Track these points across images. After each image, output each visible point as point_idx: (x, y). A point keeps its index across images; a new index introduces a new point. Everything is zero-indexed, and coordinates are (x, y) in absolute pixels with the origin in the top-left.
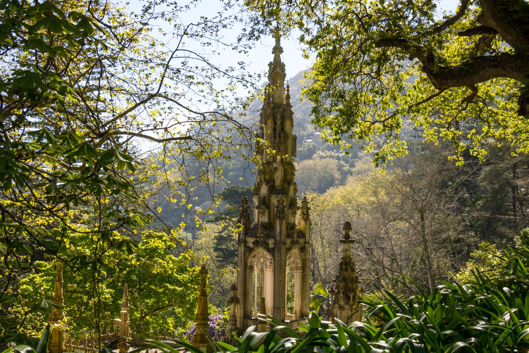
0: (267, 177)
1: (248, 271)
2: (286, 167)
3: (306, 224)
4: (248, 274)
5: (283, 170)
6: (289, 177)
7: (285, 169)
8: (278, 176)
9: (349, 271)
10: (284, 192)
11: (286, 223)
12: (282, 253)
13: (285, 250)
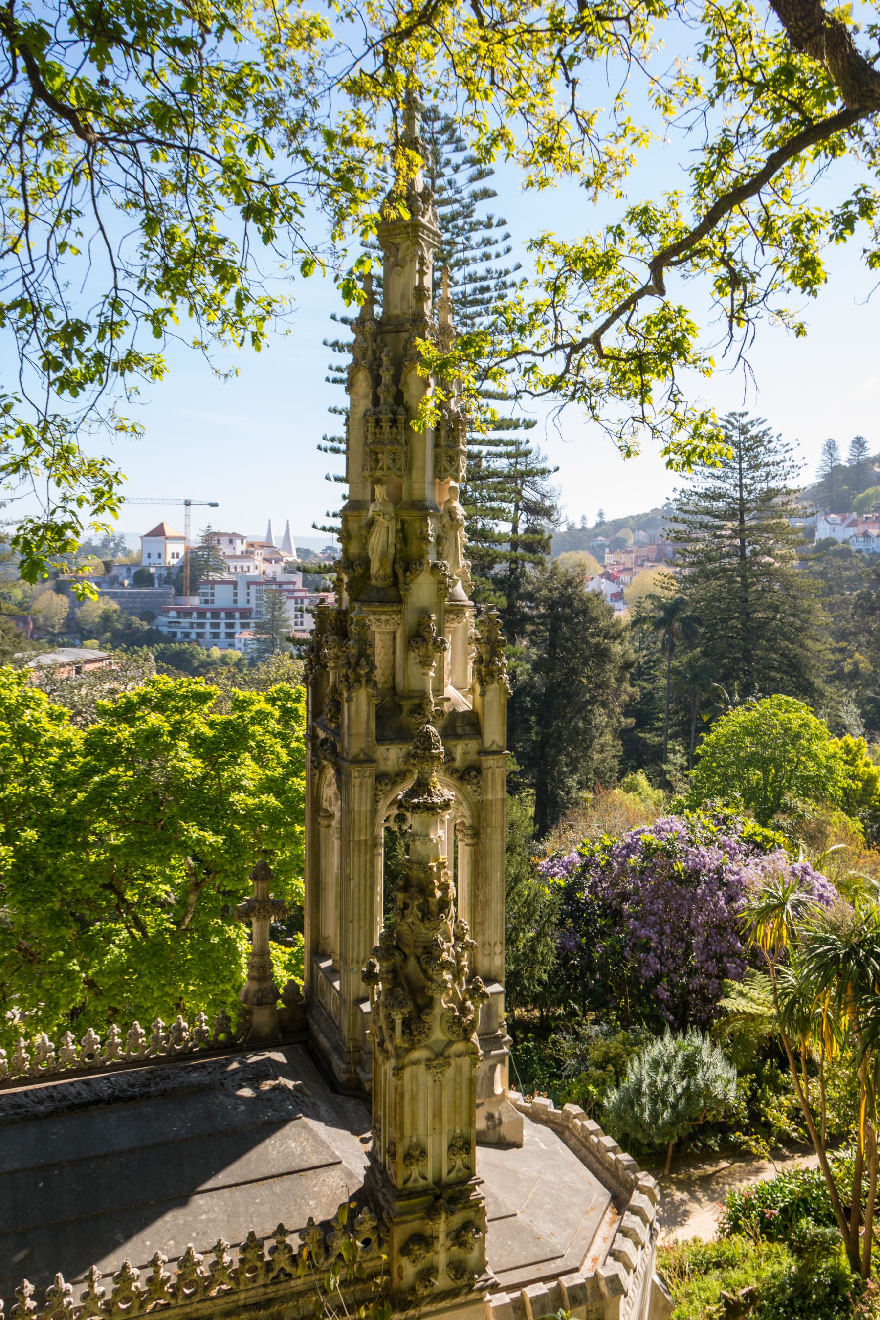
0: (354, 549)
1: (323, 822)
2: (406, 516)
3: (483, 694)
4: (322, 830)
5: (393, 526)
6: (414, 548)
7: (403, 523)
8: (380, 541)
10: (392, 594)
11: (369, 697)
12: (355, 793)
13: (369, 782)
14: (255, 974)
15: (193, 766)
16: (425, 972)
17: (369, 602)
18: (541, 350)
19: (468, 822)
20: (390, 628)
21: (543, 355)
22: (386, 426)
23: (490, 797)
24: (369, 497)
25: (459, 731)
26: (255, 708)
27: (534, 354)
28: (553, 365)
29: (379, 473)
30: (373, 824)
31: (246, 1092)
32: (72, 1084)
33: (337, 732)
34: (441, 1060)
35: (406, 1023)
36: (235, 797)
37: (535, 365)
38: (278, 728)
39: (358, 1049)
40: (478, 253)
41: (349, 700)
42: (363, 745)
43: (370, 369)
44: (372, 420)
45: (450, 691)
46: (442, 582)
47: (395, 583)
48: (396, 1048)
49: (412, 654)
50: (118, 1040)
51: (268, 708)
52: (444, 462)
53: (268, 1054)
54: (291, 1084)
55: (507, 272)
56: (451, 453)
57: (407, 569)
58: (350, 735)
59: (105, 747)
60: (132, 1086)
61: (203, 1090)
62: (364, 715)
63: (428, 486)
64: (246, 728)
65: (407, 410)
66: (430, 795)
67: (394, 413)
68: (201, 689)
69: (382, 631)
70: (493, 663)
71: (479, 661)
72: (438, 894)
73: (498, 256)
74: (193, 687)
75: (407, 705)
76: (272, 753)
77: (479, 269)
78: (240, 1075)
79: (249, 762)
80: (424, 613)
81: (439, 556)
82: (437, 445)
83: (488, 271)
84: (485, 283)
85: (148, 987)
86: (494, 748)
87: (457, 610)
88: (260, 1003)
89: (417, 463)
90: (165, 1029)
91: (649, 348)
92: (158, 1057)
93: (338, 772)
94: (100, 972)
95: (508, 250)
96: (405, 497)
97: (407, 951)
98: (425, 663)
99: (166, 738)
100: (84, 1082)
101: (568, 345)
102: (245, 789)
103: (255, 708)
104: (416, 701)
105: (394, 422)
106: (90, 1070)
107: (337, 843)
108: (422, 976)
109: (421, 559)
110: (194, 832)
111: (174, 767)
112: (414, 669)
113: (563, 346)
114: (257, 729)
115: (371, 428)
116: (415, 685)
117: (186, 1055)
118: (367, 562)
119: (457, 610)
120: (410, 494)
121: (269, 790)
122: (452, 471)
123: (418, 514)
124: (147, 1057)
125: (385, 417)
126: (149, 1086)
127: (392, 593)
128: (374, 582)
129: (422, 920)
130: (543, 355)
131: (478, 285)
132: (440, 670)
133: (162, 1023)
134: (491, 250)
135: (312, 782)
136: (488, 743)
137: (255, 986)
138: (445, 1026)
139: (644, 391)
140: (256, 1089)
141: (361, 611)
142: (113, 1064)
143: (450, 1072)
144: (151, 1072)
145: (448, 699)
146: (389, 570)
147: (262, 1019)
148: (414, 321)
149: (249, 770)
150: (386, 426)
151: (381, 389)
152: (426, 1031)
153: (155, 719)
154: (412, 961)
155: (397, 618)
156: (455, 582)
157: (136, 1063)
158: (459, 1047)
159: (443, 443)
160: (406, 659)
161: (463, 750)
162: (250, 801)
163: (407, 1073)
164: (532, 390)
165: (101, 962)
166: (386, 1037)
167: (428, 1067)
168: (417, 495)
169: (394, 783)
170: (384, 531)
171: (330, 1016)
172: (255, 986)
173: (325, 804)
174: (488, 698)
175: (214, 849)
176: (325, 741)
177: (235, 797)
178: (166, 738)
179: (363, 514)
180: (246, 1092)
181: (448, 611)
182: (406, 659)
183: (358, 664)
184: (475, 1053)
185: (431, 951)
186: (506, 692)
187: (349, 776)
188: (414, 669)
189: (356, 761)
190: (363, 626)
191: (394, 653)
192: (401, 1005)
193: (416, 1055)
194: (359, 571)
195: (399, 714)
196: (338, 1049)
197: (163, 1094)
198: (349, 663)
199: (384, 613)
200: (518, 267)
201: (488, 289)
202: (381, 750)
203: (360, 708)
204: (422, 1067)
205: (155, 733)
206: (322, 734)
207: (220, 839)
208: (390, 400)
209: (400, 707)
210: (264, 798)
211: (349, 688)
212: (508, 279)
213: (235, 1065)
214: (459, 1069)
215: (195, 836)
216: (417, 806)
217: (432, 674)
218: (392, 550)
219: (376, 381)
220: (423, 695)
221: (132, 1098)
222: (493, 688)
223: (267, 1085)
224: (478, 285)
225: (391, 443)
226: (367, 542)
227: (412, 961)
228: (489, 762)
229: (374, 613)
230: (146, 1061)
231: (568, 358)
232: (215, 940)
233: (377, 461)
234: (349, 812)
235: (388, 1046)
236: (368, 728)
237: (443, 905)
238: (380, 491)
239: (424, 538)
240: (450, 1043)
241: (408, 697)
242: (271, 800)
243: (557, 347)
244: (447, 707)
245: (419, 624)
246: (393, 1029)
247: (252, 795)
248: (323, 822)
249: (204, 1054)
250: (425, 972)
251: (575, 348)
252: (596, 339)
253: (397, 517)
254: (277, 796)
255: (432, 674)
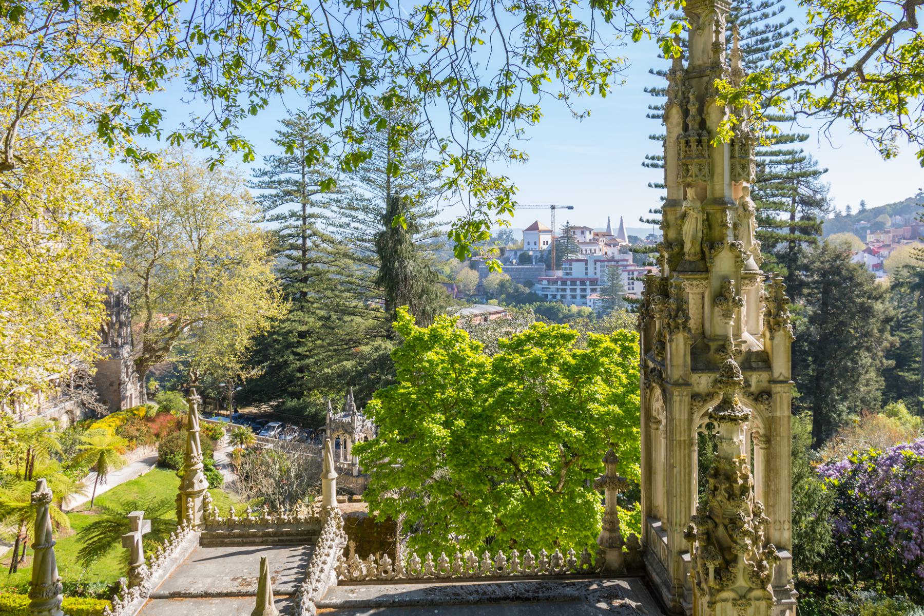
1: (654, 426)
2: (710, 209)
5: (701, 217)
6: (716, 233)
7: (708, 214)
8: (691, 229)
9: (722, 495)
11: (686, 339)
12: (676, 406)
13: (687, 399)
14: (607, 526)
15: (563, 384)
16: (731, 536)
17: (684, 271)
18: (814, 80)
19: (762, 432)
20: (700, 290)
21: (815, 84)
22: (693, 145)
23: (778, 414)
24: (682, 197)
25: (754, 365)
26: (603, 345)
27: (808, 84)
28: (824, 91)
29: (689, 180)
30: (690, 429)
31: (603, 605)
32: (489, 585)
33: (663, 364)
34: (744, 601)
35: (717, 571)
36: (591, 406)
37: (808, 93)
38: (620, 359)
39: (681, 586)
40: (758, 14)
41: (671, 341)
42: (681, 373)
43: (681, 105)
44: (683, 141)
45: (746, 336)
46: (738, 257)
47: (703, 258)
48: (710, 588)
49: (717, 309)
50: (517, 560)
51: (613, 346)
52: (738, 169)
53: (617, 582)
54: (634, 604)
55: (782, 26)
56: (743, 162)
57: (712, 247)
58: (672, 366)
59: (505, 369)
60: (528, 591)
61: (573, 600)
62: (682, 352)
63: (726, 187)
64: (597, 359)
65: (709, 132)
66: (733, 409)
67: (700, 135)
68: (566, 332)
69: (694, 292)
70: (780, 316)
71: (768, 314)
72: (740, 482)
73: (774, 14)
74: (561, 330)
75: (713, 346)
76: (616, 377)
77: (760, 25)
78: (599, 593)
79: (600, 382)
80: (725, 280)
81: (736, 237)
82: (732, 157)
83: (767, 27)
84: (764, 36)
85: (535, 528)
86: (782, 378)
87: (751, 277)
88: (611, 547)
89: (718, 170)
90: (547, 557)
91: (905, 71)
92: (543, 575)
93: (664, 391)
94: (505, 515)
95: (782, 9)
96: (709, 196)
97: (717, 520)
98: (727, 315)
99: (544, 364)
100: (497, 585)
101: (835, 74)
102: (598, 401)
103: (603, 345)
104: (721, 343)
105: (699, 142)
106: (500, 577)
107: (663, 441)
108: (729, 540)
109: (722, 240)
110: (565, 428)
111: (550, 383)
112: (718, 319)
113: (831, 76)
114: (605, 360)
115: (683, 148)
116: (719, 331)
117: (561, 576)
118: (682, 244)
119: (751, 277)
120: (713, 193)
121: (615, 402)
122: (744, 175)
123: (718, 207)
124: (536, 574)
125: (693, 139)
126: (538, 592)
127: (701, 265)
128: (687, 257)
129: (728, 499)
130: (815, 84)
131: (759, 37)
132: (738, 320)
133: (546, 553)
134: (769, 10)
135: (645, 398)
136: (776, 375)
137: (607, 535)
138: (747, 577)
139: (901, 104)
140: (610, 604)
141: (678, 278)
142: (515, 576)
143: (751, 610)
144: (539, 584)
145: (745, 342)
146: (698, 249)
147: (613, 557)
148: (713, 68)
149: (600, 388)
150: (693, 145)
151: (689, 119)
152: (733, 579)
153: (537, 351)
154: (721, 529)
155: (704, 283)
156: (748, 257)
157: (529, 577)
158: (758, 593)
159: (737, 155)
160: (712, 313)
161: (757, 379)
162: (601, 409)
163: (718, 606)
164: (807, 110)
165: (505, 509)
166: (702, 580)
167: (734, 605)
168: (718, 194)
169: (705, 401)
170: (694, 220)
171: (660, 561)
172: (607, 535)
173: (654, 414)
174: (776, 341)
175: (578, 440)
176: (653, 370)
177: (591, 406)
178: (544, 364)
179: (679, 209)
180: (603, 605)
181: (744, 278)
182: (712, 313)
183: (676, 316)
184: (770, 599)
185: (735, 522)
186: (790, 337)
187: (672, 394)
188: (718, 319)
189: (677, 384)
190: (680, 289)
191: (703, 308)
192: (713, 558)
193: (725, 595)
194: (676, 249)
195: (708, 352)
196: (667, 584)
197: (548, 599)
198: (670, 315)
199: (695, 279)
200: (791, 21)
201: (767, 40)
202: (695, 377)
203: (679, 348)
204: (730, 604)
205: (536, 361)
206: (651, 365)
207: (581, 433)
208: (697, 126)
209: (708, 347)
210: (611, 407)
211: (670, 333)
212: (783, 31)
213: (594, 586)
214: (758, 609)
215: (564, 430)
216: (723, 418)
217: (732, 323)
218: (700, 234)
219: (686, 113)
220: (725, 338)
221: (527, 599)
222: (780, 334)
223: (617, 603)
224: (759, 37)
225: (698, 157)
226: (681, 229)
227: (721, 529)
228: (777, 388)
229: (688, 279)
230: (536, 576)
231: (836, 84)
232: (579, 501)
233: (688, 171)
234: (672, 420)
235: (704, 585)
236: (685, 361)
237: (744, 490)
238: (690, 192)
239: (724, 225)
240: (751, 590)
241: (715, 340)
242: (616, 409)
243: (826, 77)
244: (744, 348)
245: (722, 287)
246: (707, 574)
247: (603, 405)
248: (654, 426)
249: (573, 576)
250: (731, 536)
251: (841, 76)
252: (859, 68)
253: (703, 210)
254: (620, 406)
255: (732, 323)
